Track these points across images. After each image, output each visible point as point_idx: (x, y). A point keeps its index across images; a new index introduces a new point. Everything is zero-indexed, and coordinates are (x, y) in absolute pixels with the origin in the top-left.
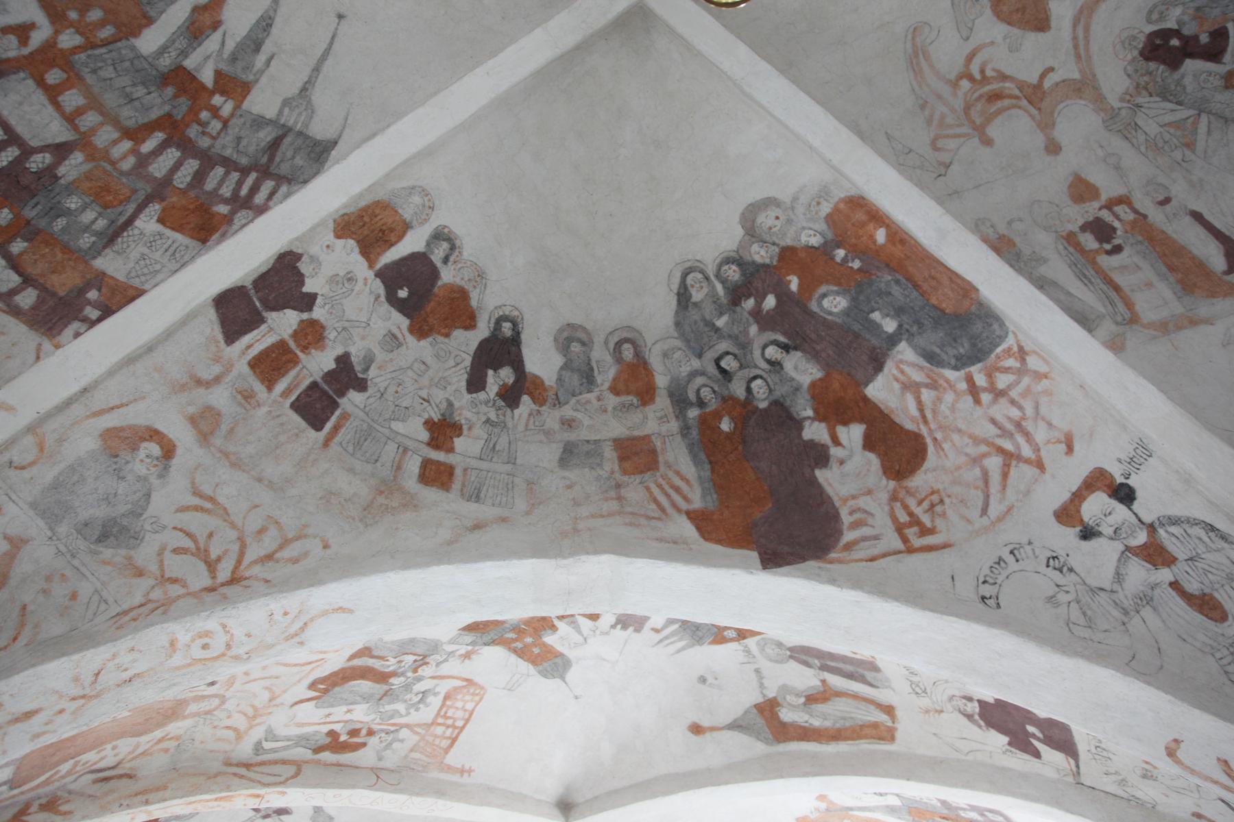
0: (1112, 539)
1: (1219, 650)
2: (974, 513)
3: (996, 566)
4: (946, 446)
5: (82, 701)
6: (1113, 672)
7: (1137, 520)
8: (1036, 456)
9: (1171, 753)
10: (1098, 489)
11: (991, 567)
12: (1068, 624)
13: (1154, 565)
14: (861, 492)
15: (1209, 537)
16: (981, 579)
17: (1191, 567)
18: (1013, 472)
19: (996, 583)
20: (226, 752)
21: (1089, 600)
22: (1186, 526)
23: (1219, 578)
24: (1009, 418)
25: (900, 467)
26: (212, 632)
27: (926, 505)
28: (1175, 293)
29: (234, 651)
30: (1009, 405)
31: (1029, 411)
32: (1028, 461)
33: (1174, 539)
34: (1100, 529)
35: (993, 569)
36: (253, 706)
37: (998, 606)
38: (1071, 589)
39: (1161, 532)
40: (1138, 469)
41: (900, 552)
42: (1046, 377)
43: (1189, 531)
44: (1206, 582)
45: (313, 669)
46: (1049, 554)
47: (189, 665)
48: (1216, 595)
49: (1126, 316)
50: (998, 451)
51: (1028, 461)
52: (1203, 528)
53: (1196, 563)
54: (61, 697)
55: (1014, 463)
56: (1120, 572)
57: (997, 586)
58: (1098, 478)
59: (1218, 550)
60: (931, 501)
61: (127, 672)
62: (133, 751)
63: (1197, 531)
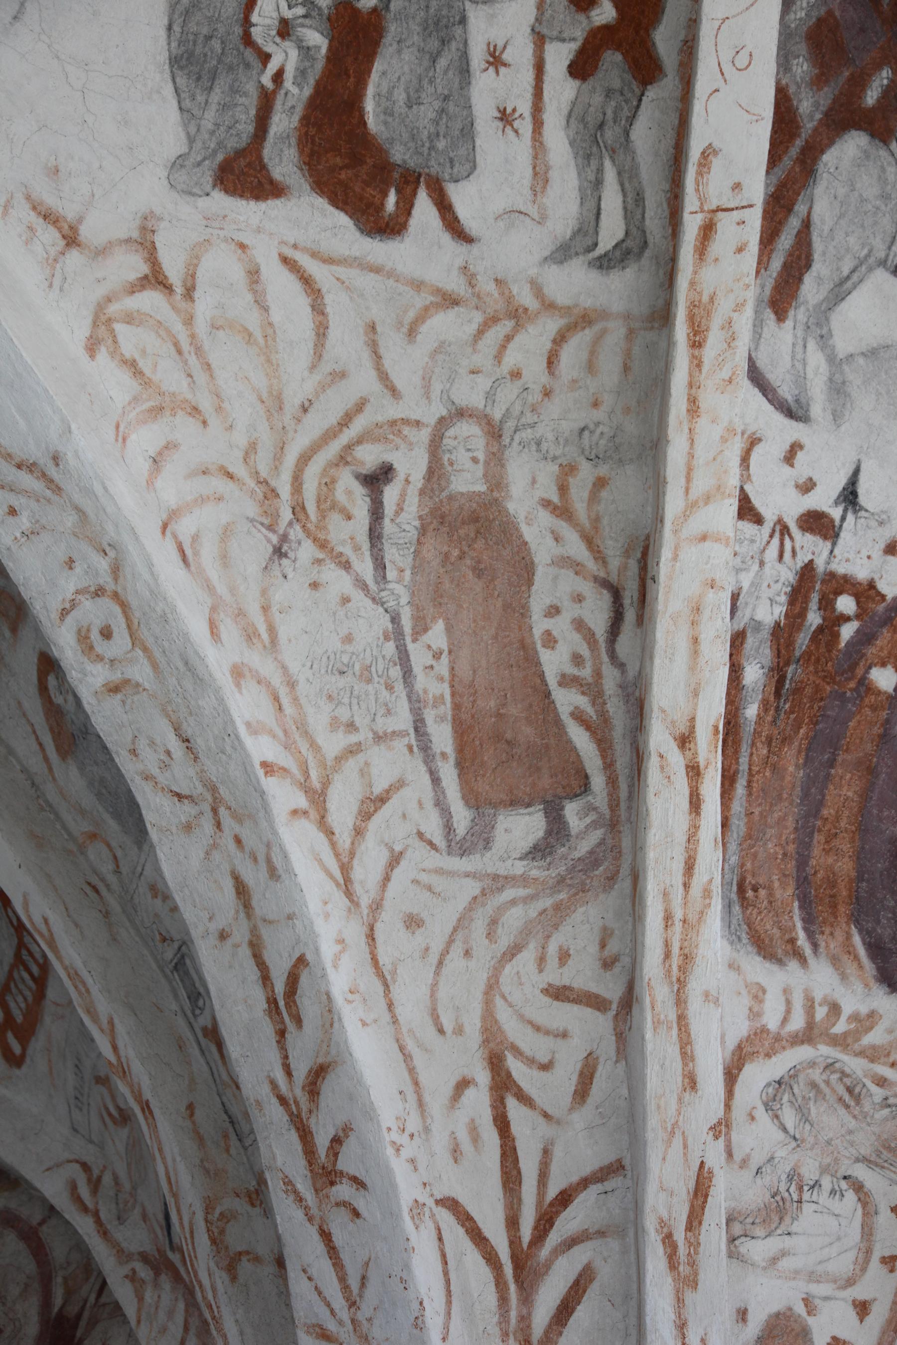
5: (222, 811)
20: (631, 334)
26: (79, 631)
29: (106, 579)
36: (480, 333)
45: (329, 261)
47: (145, 650)
54: (215, 846)
61: (172, 750)
62: (577, 568)
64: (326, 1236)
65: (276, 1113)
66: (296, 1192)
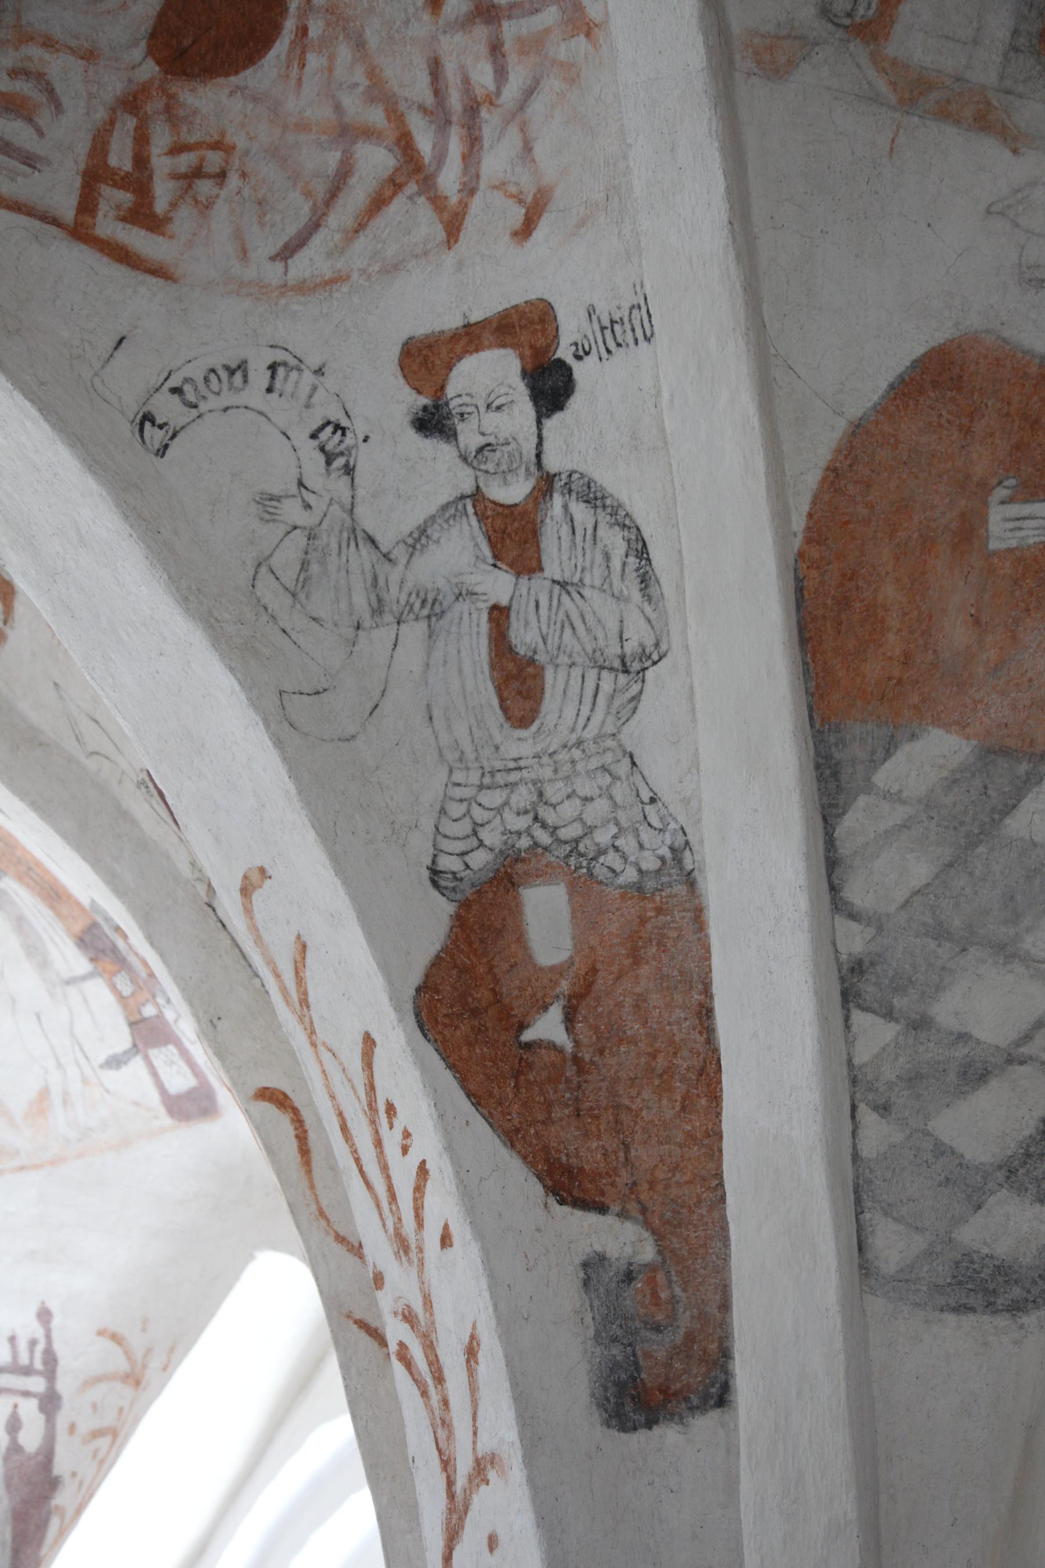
0: (464, 459)
1: (468, 769)
2: (264, 245)
3: (224, 375)
4: (314, 61)
6: (237, 687)
7: (533, 452)
8: (460, 202)
9: (246, 891)
10: (514, 346)
11: (213, 371)
12: (259, 565)
13: (496, 557)
14: (73, 43)
15: (624, 564)
16: (173, 382)
17: (551, 600)
18: (397, 206)
19: (196, 406)
21: (334, 546)
22: (603, 518)
23: (578, 648)
24: (466, 81)
25: (194, 42)
27: (185, 161)
28: (1016, 32)
30: (483, 50)
31: (511, 92)
32: (438, 202)
33: (565, 530)
34: (460, 427)
35: (213, 377)
37: (162, 451)
38: (319, 505)
39: (558, 500)
40: (609, 351)
41: (55, 222)
42: (588, 35)
43: (601, 532)
44: (553, 641)
46: (336, 414)
48: (549, 675)
49: (861, 11)
50: (398, 141)
51: (438, 202)
52: (629, 541)
53: (565, 598)
55: (412, 188)
56: (429, 532)
57: (194, 413)
58: (532, 322)
59: (618, 598)
60: (202, 160)
63: (615, 541)
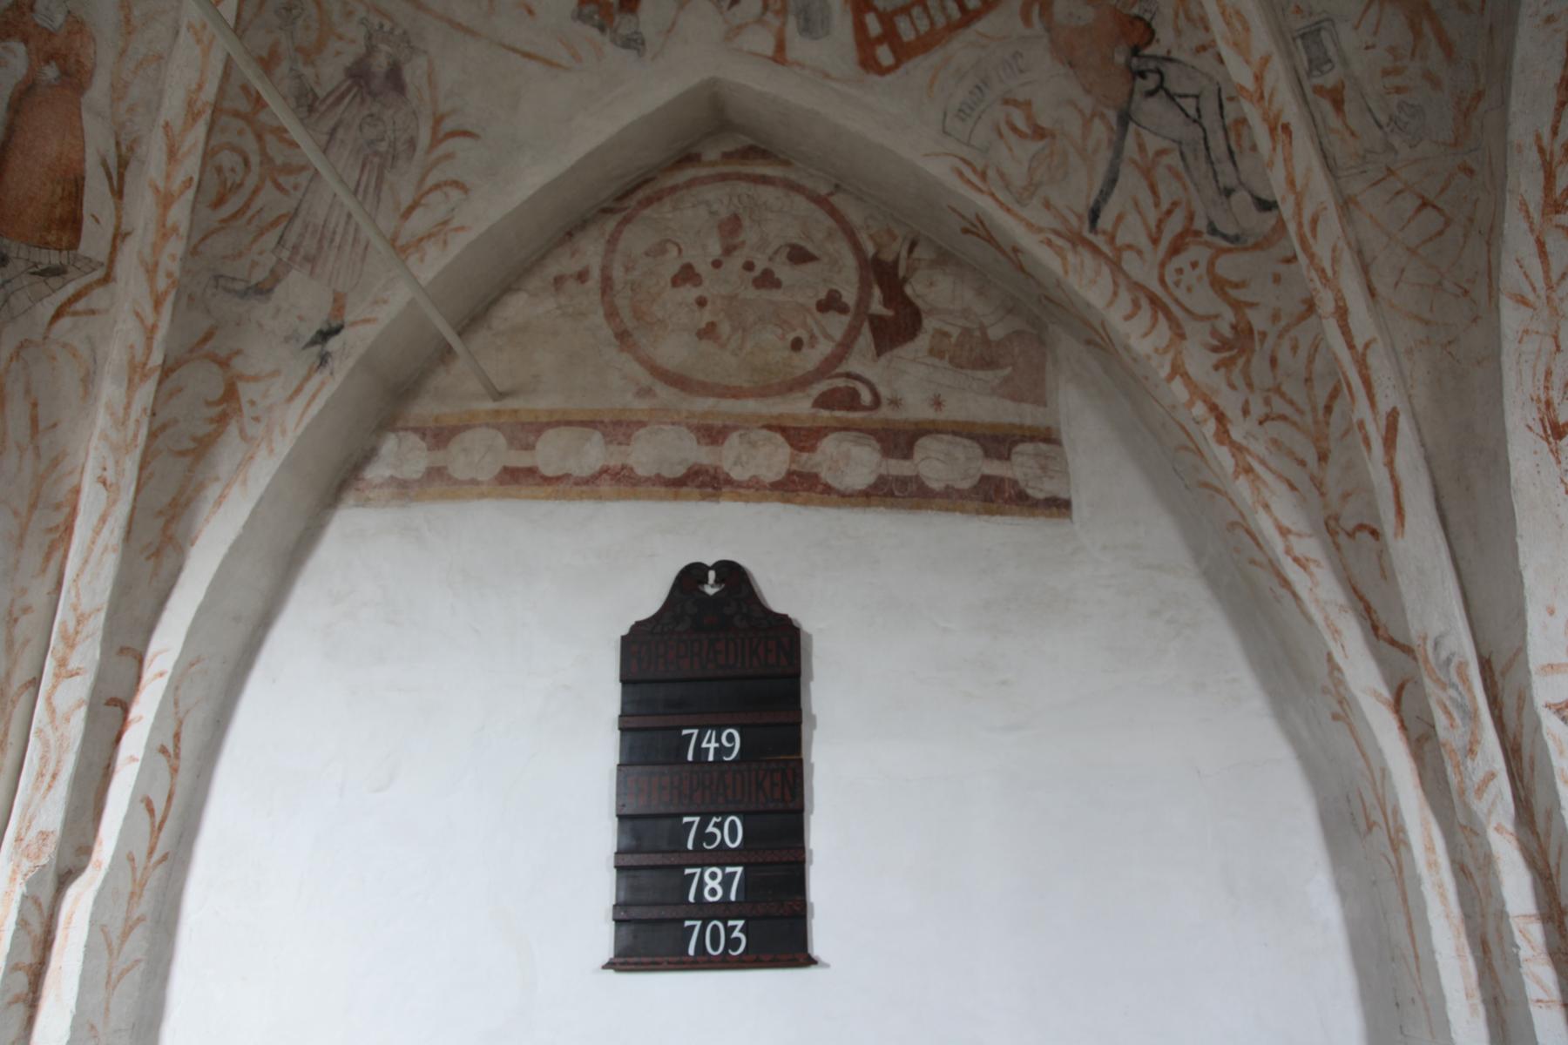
64: (1541, 244)
65: (1533, 156)
66: (1527, 212)
